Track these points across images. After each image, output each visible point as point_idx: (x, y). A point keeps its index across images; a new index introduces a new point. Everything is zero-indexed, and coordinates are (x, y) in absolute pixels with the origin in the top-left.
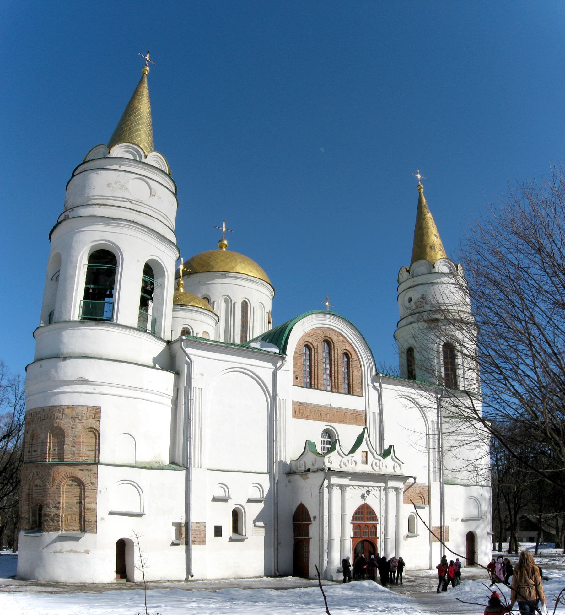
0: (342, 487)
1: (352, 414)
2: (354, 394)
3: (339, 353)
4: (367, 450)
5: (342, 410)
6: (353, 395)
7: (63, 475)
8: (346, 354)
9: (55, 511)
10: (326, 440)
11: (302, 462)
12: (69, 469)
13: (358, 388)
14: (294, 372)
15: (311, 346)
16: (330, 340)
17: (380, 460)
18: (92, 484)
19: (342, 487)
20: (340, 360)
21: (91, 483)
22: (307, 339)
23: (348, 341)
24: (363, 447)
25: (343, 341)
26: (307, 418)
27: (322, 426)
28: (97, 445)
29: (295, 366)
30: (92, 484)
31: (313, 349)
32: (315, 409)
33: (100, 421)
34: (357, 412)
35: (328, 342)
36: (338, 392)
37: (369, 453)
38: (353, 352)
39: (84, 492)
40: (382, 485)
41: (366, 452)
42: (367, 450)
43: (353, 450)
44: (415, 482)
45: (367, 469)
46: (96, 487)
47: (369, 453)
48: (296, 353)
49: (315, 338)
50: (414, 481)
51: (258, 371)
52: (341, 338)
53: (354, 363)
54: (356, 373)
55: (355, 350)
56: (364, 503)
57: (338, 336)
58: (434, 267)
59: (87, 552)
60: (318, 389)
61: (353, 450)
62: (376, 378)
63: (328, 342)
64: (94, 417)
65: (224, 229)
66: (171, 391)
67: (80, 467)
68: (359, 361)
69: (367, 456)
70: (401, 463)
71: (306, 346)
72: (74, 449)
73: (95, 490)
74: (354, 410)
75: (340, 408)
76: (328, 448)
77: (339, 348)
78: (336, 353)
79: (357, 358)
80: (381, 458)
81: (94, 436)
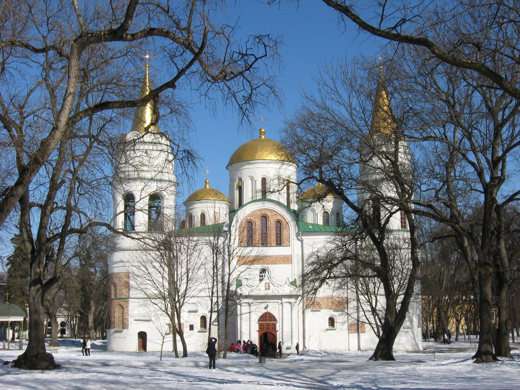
0: (249, 304)
1: (281, 258)
4: (269, 282)
8: (279, 222)
12: (118, 301)
19: (249, 303)
22: (249, 218)
35: (265, 218)
36: (271, 246)
38: (283, 220)
40: (280, 301)
42: (269, 282)
45: (269, 293)
47: (270, 284)
52: (274, 213)
54: (285, 233)
59: (125, 338)
62: (298, 235)
65: (262, 120)
73: (128, 310)
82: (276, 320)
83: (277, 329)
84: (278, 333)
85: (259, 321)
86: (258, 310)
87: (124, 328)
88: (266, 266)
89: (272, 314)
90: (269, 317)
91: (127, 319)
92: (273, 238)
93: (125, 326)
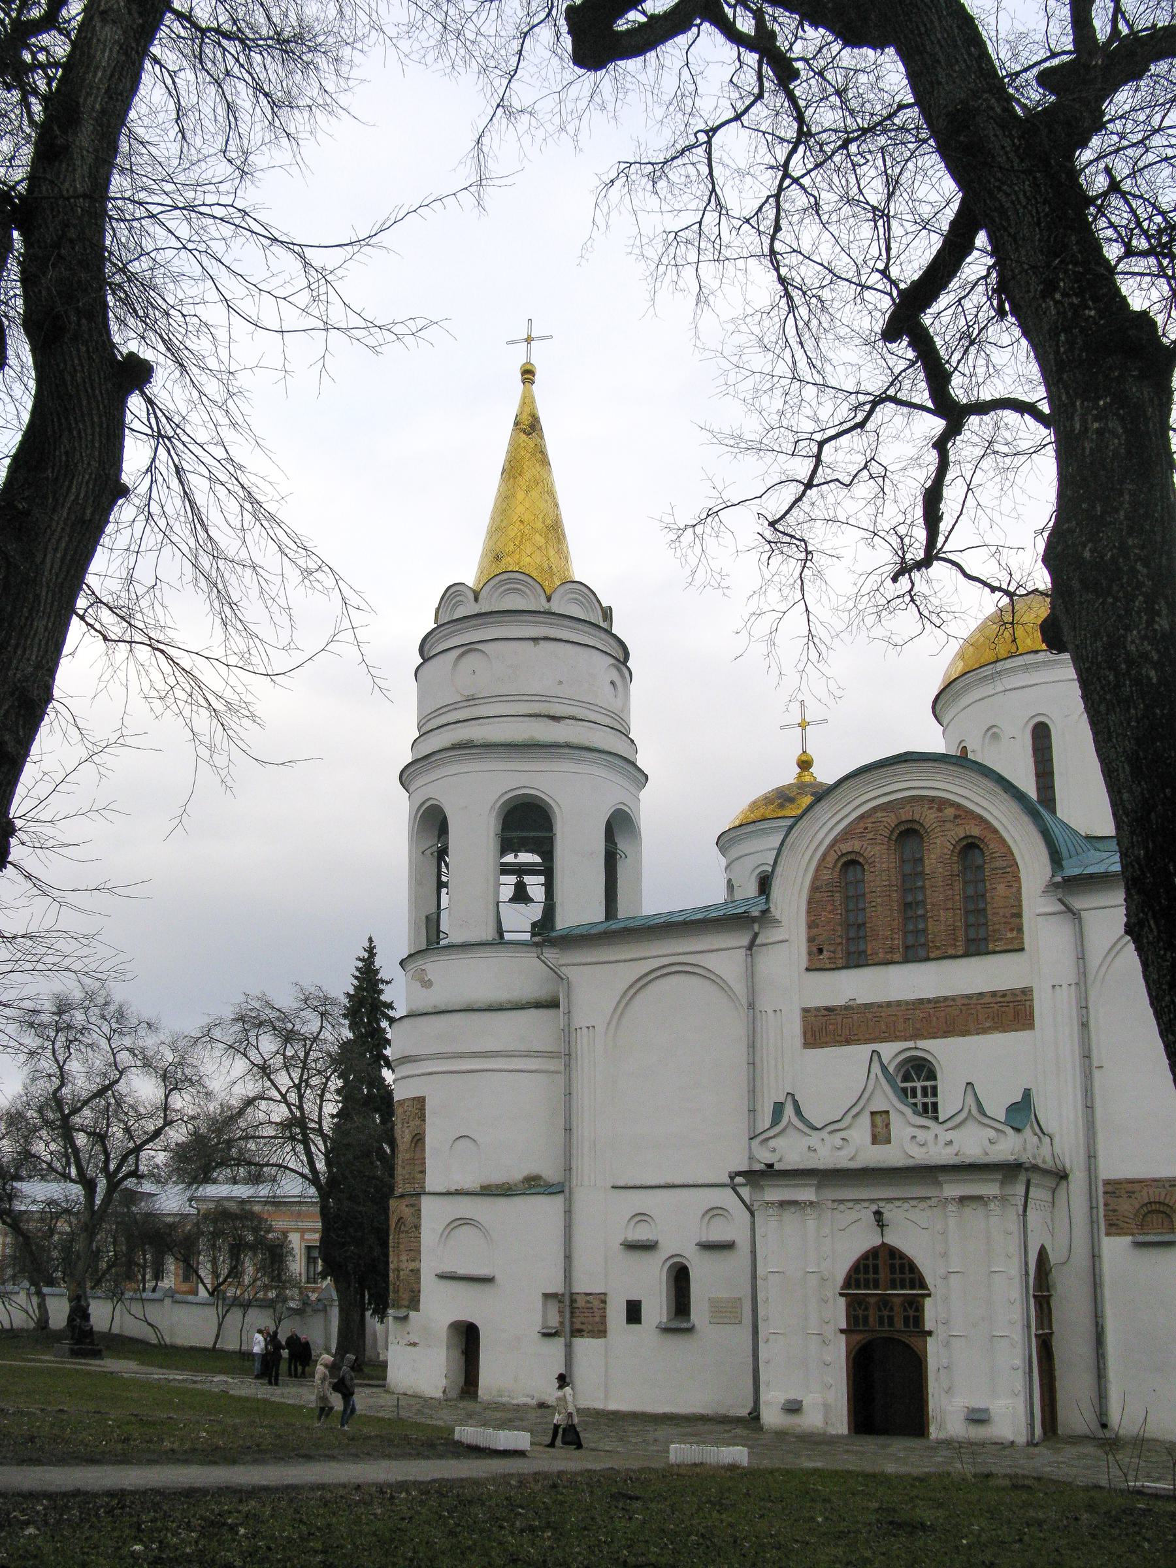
1: (986, 1006)
2: (997, 949)
5: (953, 999)
6: (995, 952)
8: (970, 848)
13: (1012, 930)
14: (811, 940)
15: (861, 860)
16: (917, 827)
22: (846, 847)
25: (956, 817)
29: (811, 925)
32: (870, 1016)
34: (1004, 996)
41: (887, 1112)
47: (893, 1116)
48: (814, 888)
49: (870, 836)
51: (712, 962)
55: (996, 831)
56: (877, 1242)
57: (940, 810)
68: (1013, 854)
75: (946, 998)
82: (922, 1285)
83: (928, 1326)
85: (847, 1284)
88: (921, 1044)
89: (902, 1256)
90: (892, 1267)
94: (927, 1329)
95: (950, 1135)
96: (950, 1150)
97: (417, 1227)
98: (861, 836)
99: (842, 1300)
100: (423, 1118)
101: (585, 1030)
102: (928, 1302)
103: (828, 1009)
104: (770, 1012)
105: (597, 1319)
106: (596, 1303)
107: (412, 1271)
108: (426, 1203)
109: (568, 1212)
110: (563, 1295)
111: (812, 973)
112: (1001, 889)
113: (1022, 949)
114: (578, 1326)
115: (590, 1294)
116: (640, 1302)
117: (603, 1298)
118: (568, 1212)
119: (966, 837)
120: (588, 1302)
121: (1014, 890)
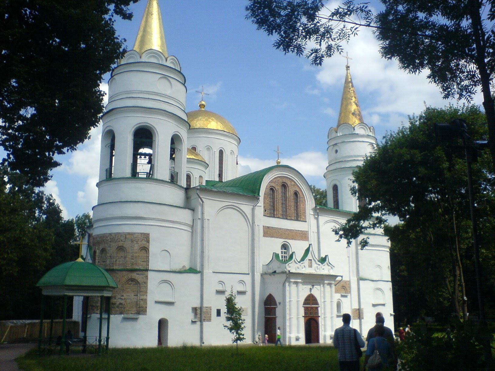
1: (300, 234)
2: (301, 220)
3: (292, 193)
4: (311, 258)
5: (293, 230)
6: (300, 221)
7: (126, 277)
8: (296, 194)
9: (120, 301)
10: (283, 251)
11: (270, 266)
15: (274, 189)
17: (319, 265)
18: (145, 283)
20: (292, 198)
21: (144, 283)
22: (273, 185)
23: (297, 185)
24: (309, 257)
25: (294, 185)
26: (272, 237)
27: (279, 242)
28: (148, 257)
29: (264, 203)
30: (145, 283)
31: (275, 191)
33: (149, 242)
35: (284, 186)
37: (313, 260)
38: (300, 192)
39: (140, 288)
41: (311, 260)
42: (312, 259)
43: (303, 259)
44: (342, 279)
46: (147, 285)
47: (313, 260)
49: (277, 183)
50: (341, 279)
52: (293, 183)
53: (301, 199)
55: (301, 191)
56: (310, 293)
58: (354, 129)
60: (278, 218)
61: (303, 259)
63: (284, 186)
64: (145, 240)
66: (189, 221)
67: (137, 273)
68: (304, 198)
69: (311, 263)
70: (332, 267)
71: (272, 189)
72: (133, 261)
73: (146, 287)
74: (301, 231)
76: (284, 256)
77: (291, 189)
78: (290, 193)
79: (303, 196)
80: (320, 264)
81: (146, 252)
82: (317, 304)
84: (320, 318)
85: (304, 304)
86: (304, 291)
87: (138, 313)
91: (145, 301)
92: (292, 211)
93: (141, 310)
94: (319, 315)
95: (323, 267)
96: (323, 271)
97: (146, 283)
98: (275, 183)
99: (303, 308)
100: (148, 241)
101: (206, 220)
102: (319, 309)
103: (268, 227)
104: (256, 225)
105: (209, 315)
106: (209, 310)
107: (142, 300)
108: (150, 274)
109: (202, 280)
110: (199, 308)
111: (265, 217)
112: (302, 206)
113: (306, 222)
114: (204, 318)
115: (208, 307)
116: (220, 309)
117: (210, 308)
118: (202, 280)
119: (296, 191)
120: (207, 310)
121: (304, 206)
